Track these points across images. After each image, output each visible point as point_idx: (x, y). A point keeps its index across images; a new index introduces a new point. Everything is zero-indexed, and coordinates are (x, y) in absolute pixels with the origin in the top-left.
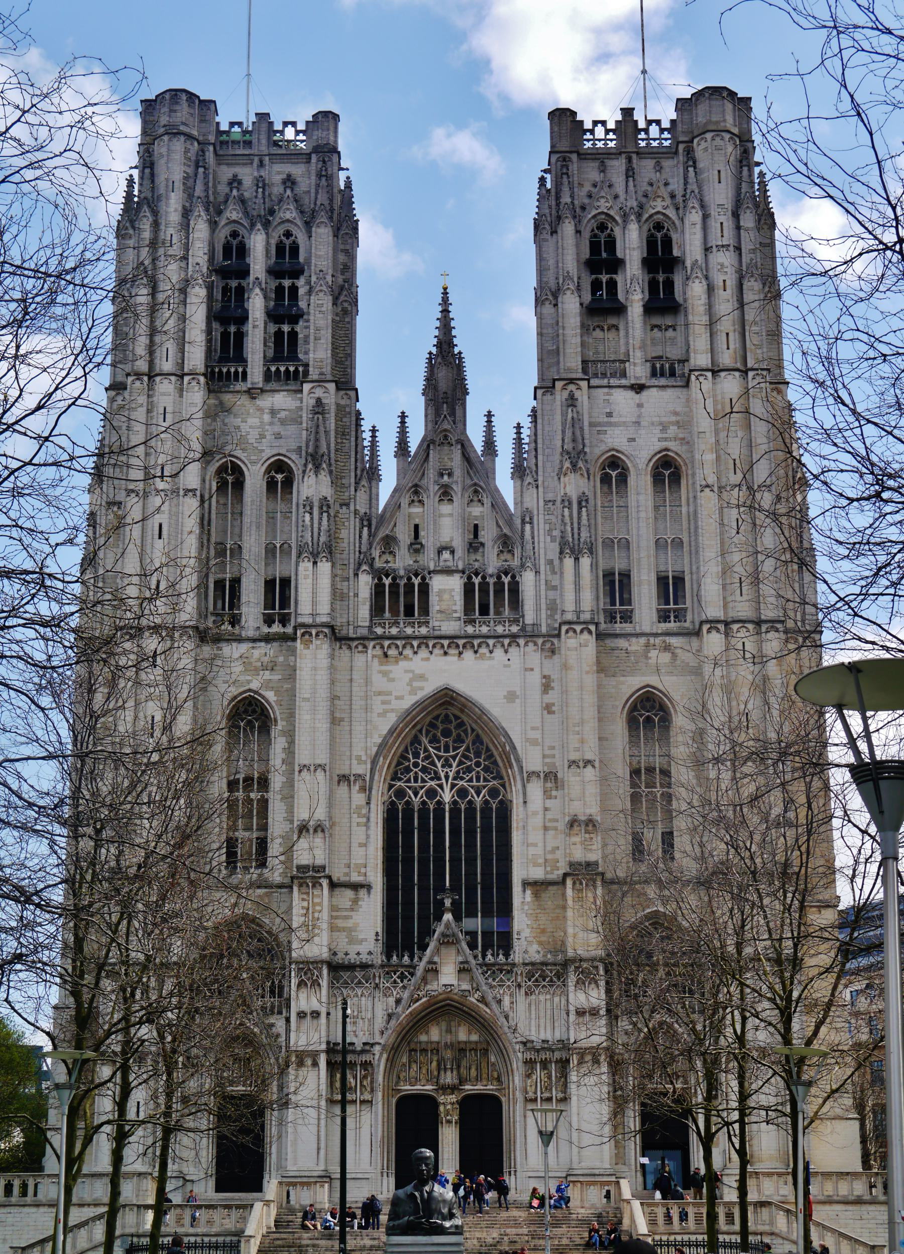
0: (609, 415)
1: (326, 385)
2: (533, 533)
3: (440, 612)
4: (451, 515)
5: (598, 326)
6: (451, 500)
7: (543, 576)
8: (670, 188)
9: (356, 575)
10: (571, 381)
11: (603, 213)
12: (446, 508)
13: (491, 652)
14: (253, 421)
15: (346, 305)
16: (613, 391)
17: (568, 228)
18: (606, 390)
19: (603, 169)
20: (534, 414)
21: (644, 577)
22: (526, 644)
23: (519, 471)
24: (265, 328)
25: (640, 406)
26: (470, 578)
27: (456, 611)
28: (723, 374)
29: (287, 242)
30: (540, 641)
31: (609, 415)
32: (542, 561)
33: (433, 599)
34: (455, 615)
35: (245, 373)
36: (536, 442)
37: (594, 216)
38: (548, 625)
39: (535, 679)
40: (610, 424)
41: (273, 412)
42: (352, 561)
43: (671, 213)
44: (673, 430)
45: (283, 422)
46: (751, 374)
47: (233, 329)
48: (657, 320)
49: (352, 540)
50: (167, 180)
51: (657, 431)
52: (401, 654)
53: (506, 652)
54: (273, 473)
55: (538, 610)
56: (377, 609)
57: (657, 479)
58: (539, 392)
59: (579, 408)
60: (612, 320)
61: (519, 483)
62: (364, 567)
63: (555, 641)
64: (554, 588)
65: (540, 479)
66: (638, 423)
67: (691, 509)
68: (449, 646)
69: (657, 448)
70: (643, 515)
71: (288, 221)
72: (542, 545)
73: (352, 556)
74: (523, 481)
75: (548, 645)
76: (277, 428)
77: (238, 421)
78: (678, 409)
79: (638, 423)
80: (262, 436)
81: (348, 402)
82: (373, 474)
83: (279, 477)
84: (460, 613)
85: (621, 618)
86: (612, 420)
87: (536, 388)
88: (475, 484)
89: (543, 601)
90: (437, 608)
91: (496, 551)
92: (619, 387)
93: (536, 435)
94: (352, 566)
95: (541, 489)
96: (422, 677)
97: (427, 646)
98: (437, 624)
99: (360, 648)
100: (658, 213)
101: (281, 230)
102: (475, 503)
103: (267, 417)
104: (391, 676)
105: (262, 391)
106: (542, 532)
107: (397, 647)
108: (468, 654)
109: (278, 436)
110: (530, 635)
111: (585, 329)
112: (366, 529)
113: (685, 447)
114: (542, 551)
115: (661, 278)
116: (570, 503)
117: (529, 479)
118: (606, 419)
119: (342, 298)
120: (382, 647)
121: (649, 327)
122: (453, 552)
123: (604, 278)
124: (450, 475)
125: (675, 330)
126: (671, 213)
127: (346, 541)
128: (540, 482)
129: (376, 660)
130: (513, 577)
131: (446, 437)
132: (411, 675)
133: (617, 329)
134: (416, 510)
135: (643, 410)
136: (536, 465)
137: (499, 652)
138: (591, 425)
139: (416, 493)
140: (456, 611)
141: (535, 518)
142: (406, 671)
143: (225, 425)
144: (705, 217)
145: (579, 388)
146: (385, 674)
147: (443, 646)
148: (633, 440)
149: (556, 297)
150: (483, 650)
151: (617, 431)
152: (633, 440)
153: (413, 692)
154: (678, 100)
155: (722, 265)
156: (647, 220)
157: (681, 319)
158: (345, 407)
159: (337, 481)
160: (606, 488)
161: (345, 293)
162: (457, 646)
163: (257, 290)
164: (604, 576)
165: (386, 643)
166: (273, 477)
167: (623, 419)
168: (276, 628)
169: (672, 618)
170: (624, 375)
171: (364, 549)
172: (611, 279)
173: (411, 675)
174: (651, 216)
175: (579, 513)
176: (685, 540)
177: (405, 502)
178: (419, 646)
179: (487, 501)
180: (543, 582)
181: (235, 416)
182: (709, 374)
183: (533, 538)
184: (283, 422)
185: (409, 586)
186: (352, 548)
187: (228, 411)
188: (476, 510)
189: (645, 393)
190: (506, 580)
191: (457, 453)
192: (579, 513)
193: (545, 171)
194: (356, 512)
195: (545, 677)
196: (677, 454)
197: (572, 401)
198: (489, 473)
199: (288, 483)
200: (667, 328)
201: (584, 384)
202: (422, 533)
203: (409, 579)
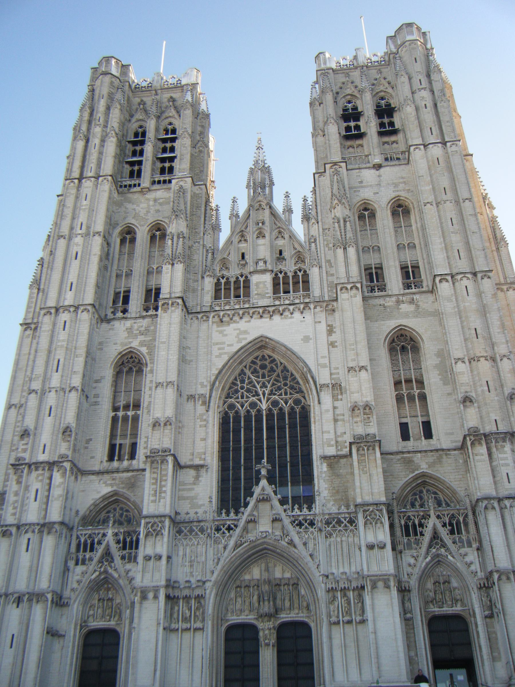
0: (361, 182)
1: (186, 179)
2: (316, 246)
3: (257, 294)
4: (264, 245)
5: (351, 146)
6: (264, 237)
7: (324, 269)
8: (387, 80)
9: (203, 278)
10: (335, 164)
11: (349, 95)
12: (261, 241)
13: (292, 314)
14: (144, 205)
15: (201, 148)
16: (363, 170)
17: (329, 98)
18: (358, 171)
19: (348, 75)
20: (314, 191)
21: (392, 263)
22: (315, 308)
23: (306, 218)
24: (154, 163)
25: (379, 176)
26: (276, 275)
27: (268, 293)
28: (430, 146)
29: (170, 127)
30: (325, 304)
31: (361, 182)
32: (323, 260)
33: (253, 287)
34: (267, 295)
35: (139, 185)
36: (316, 202)
37: (344, 97)
38: (329, 296)
39: (323, 327)
40: (362, 187)
41: (155, 200)
42: (200, 270)
43: (390, 90)
44: (401, 186)
45: (161, 204)
46: (448, 144)
47: (136, 168)
48: (386, 139)
49: (201, 259)
50: (99, 94)
51: (392, 188)
52: (231, 319)
53: (302, 313)
54: (154, 231)
55: (322, 289)
56: (217, 296)
57: (394, 214)
58: (317, 176)
59: (341, 175)
60: (359, 142)
61: (306, 223)
62: (208, 273)
63: (335, 304)
64: (332, 275)
65: (320, 218)
66: (379, 185)
67: (419, 225)
68: (263, 313)
69: (393, 196)
70: (387, 230)
71: (170, 117)
72: (322, 252)
73: (201, 268)
74: (308, 223)
75: (330, 307)
76: (158, 207)
77: (135, 206)
78: (404, 176)
79: (379, 185)
80: (148, 212)
81: (201, 192)
82: (216, 228)
83: (158, 233)
84: (271, 294)
85: (378, 289)
86: (363, 184)
87: (314, 174)
88: (279, 227)
89: (325, 282)
90: (256, 292)
91: (293, 261)
92: (366, 168)
93: (316, 199)
94: (200, 273)
95: (320, 223)
96: (246, 332)
97: (249, 314)
98: (255, 301)
99: (205, 318)
100: (381, 91)
101: (167, 121)
102: (280, 239)
103: (151, 203)
104: (225, 333)
105: (150, 190)
106: (322, 245)
107: (229, 315)
108: (277, 318)
109: (158, 211)
110: (318, 302)
111: (343, 147)
112: (210, 255)
113: (410, 194)
114: (323, 255)
115: (386, 120)
116: (339, 222)
117: (313, 221)
118: (359, 185)
119: (199, 145)
120: (219, 316)
121: (381, 143)
122: (265, 262)
123: (352, 124)
124: (263, 223)
125: (397, 143)
126: (390, 90)
127: (197, 261)
128: (319, 220)
129: (215, 326)
130: (305, 271)
131: (260, 205)
132: (238, 331)
133: (362, 146)
134: (243, 245)
135: (382, 178)
136: (317, 212)
137: (297, 315)
138: (349, 188)
139: (242, 236)
140: (268, 293)
141: (318, 239)
142: (235, 330)
143: (126, 208)
144: (410, 79)
145: (341, 167)
146: (221, 332)
147: (259, 313)
148: (378, 193)
149: (323, 131)
150: (287, 313)
151: (366, 190)
152: (378, 193)
153: (239, 341)
154: (387, 37)
155: (423, 98)
156: (375, 95)
157: (400, 137)
158: (198, 194)
159: (192, 228)
160: (362, 223)
161: (201, 143)
162: (269, 312)
163: (150, 144)
164: (365, 270)
165: (222, 313)
166: (154, 234)
167: (370, 184)
168: (151, 312)
169: (413, 287)
170: (369, 162)
171: (209, 264)
172: (357, 125)
173: (238, 331)
174: (377, 93)
175: (345, 226)
176: (416, 242)
177: (236, 239)
178: (243, 314)
179: (286, 236)
180: (324, 272)
181: (133, 204)
182: (422, 147)
183: (317, 249)
184: (161, 204)
185: (237, 281)
186: (201, 263)
187: (130, 202)
188: (280, 242)
189: (382, 170)
190: (300, 274)
191: (267, 212)
192: (345, 226)
193: (314, 82)
194: (204, 246)
195: (329, 326)
196: (406, 198)
197: (337, 173)
198: (290, 221)
199: (163, 236)
200: (393, 142)
201: (343, 165)
202: (246, 257)
203: (237, 278)
